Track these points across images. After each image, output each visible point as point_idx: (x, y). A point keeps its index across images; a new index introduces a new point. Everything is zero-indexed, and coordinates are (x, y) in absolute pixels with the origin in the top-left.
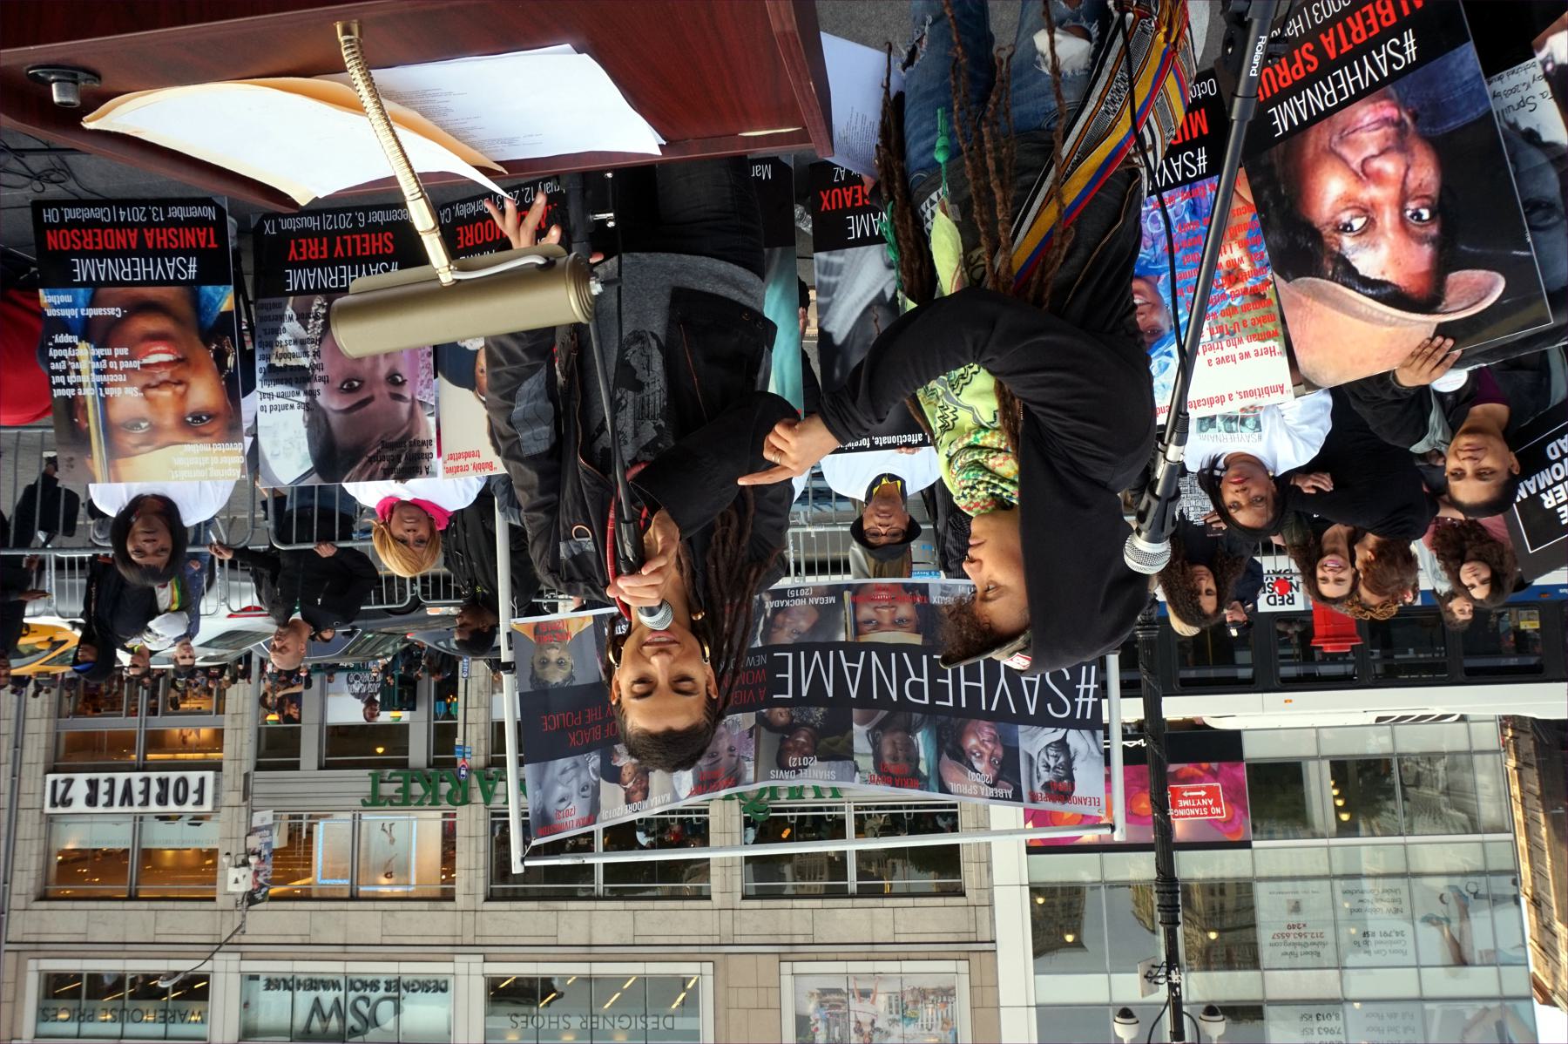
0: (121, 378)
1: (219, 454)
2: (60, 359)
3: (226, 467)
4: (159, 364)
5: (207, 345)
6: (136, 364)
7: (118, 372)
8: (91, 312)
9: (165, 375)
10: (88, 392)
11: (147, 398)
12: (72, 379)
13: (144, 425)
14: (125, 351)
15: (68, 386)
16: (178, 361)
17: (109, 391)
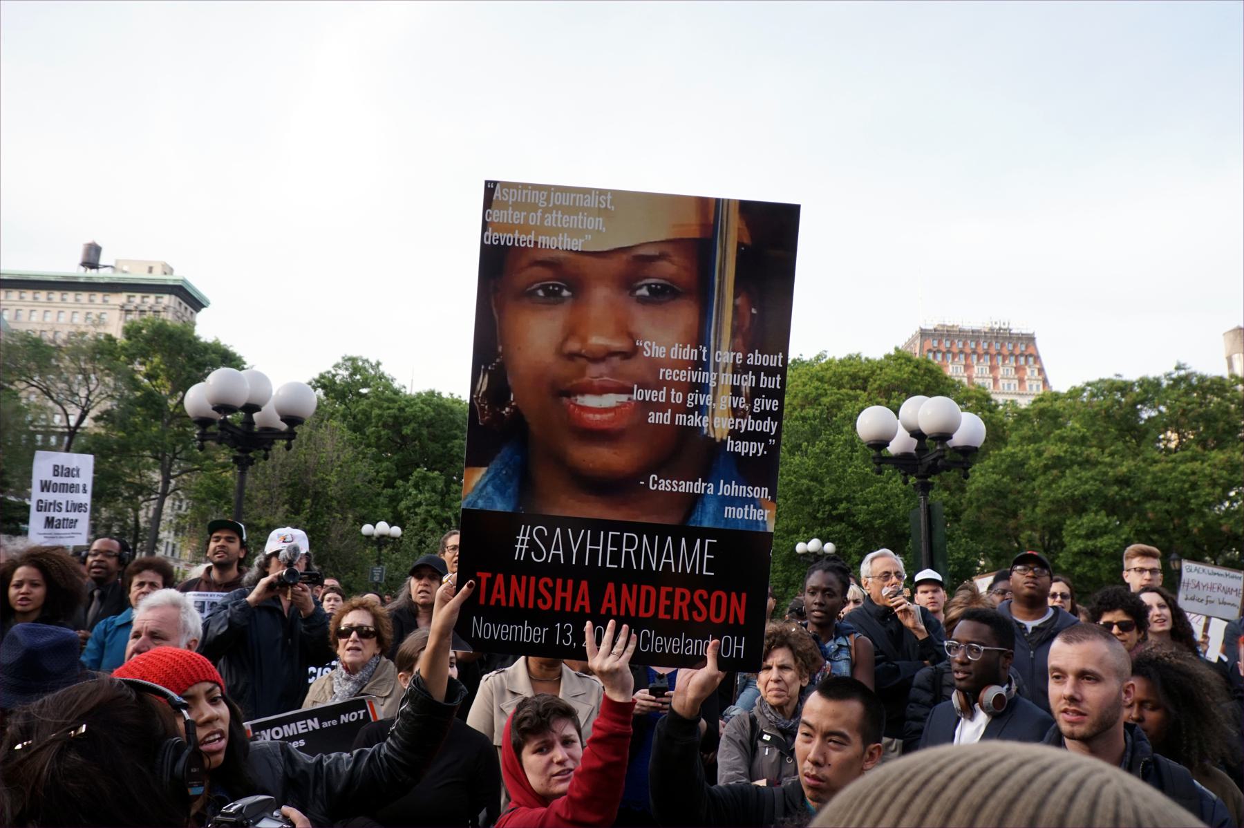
0: (668, 374)
1: (525, 229)
2: (762, 416)
3: (517, 206)
4: (602, 391)
5: (517, 414)
6: (638, 395)
7: (670, 385)
8: (698, 487)
9: (595, 372)
10: (725, 356)
11: (632, 337)
12: (747, 382)
13: (644, 292)
14: (654, 418)
15: (757, 370)
16: (571, 392)
17: (689, 354)
